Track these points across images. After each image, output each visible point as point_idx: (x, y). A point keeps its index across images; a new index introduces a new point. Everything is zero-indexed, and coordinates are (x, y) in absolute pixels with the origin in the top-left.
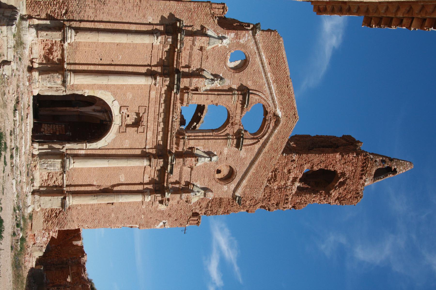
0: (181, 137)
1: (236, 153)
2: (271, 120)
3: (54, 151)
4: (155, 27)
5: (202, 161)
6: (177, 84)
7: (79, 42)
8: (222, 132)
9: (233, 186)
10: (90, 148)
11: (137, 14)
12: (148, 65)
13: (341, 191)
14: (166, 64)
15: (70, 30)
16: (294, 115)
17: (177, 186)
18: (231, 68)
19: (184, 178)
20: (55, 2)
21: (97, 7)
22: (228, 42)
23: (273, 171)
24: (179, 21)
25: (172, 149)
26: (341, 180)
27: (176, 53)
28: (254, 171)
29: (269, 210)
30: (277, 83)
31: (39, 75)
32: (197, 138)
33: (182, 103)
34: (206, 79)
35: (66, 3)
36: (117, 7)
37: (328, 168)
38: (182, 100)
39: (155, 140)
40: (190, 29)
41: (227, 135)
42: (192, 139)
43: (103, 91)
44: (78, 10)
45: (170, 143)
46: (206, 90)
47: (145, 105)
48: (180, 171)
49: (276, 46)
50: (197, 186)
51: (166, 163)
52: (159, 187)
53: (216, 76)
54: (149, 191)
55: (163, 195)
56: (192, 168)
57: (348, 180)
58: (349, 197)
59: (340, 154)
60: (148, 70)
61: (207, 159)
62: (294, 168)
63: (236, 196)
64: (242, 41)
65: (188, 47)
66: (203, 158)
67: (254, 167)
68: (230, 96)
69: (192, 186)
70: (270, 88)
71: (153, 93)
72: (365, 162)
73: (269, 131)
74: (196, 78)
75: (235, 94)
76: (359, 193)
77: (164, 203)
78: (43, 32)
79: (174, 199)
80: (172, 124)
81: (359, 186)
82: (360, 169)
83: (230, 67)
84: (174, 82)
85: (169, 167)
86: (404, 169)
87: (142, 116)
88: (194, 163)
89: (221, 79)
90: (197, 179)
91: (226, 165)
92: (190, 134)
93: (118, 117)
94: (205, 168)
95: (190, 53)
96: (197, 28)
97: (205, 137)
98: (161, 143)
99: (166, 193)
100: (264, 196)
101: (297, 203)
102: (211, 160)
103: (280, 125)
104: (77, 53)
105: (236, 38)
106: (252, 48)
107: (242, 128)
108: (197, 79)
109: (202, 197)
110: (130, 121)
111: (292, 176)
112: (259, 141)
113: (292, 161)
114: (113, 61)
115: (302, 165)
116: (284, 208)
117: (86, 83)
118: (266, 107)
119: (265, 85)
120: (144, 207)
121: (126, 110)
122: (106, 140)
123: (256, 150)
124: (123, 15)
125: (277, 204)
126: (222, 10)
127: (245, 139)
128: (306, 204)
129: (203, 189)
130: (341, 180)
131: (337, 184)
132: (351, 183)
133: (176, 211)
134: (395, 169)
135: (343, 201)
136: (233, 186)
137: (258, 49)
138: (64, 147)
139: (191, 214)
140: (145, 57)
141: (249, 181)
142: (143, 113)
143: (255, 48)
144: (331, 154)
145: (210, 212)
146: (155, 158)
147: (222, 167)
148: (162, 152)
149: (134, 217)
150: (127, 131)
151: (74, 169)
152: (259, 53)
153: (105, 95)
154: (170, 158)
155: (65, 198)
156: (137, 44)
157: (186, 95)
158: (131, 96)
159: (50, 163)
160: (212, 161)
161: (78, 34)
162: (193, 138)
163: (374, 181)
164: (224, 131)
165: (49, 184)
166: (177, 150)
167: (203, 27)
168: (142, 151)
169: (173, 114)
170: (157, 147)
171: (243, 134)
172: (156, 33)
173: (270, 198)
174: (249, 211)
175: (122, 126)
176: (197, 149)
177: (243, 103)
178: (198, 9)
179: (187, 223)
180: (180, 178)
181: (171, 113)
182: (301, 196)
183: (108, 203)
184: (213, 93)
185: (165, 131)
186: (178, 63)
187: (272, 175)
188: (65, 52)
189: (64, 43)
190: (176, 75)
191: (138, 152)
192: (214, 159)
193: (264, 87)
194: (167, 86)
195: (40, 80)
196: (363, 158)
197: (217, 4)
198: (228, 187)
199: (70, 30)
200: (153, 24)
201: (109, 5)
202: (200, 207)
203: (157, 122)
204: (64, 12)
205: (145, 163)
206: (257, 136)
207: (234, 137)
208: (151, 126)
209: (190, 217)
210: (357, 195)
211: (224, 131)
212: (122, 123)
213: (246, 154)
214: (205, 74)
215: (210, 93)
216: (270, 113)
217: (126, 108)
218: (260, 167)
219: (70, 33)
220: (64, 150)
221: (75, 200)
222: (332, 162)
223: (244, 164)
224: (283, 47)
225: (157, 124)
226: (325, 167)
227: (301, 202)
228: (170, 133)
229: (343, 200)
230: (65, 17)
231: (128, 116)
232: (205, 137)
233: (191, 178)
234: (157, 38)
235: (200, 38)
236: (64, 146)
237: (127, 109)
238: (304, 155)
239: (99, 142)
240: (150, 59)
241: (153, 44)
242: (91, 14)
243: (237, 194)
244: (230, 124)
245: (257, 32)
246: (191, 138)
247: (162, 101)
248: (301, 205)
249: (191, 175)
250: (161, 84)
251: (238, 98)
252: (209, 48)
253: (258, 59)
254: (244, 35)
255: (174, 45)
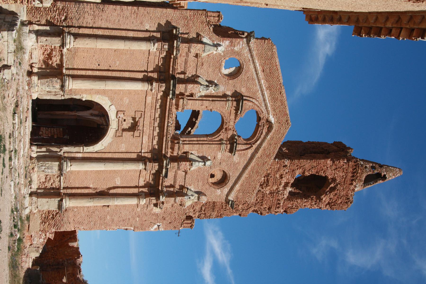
0: (176, 141)
1: (229, 157)
2: (264, 126)
3: (51, 154)
4: (152, 34)
5: (197, 166)
6: (172, 90)
7: (78, 48)
8: (216, 138)
9: (226, 190)
10: (87, 151)
11: (135, 21)
12: (145, 71)
13: (332, 196)
14: (162, 70)
15: (69, 36)
16: (287, 121)
17: (172, 189)
18: (226, 75)
19: (178, 182)
20: (55, 9)
21: (95, 14)
22: (223, 49)
23: (266, 176)
24: (176, 28)
25: (167, 153)
26: (332, 185)
27: (172, 60)
28: (247, 176)
29: (261, 214)
30: (270, 90)
31: (38, 79)
32: (192, 142)
33: (177, 109)
34: (201, 85)
35: (66, 10)
36: (115, 14)
37: (320, 174)
38: (177, 105)
39: (151, 145)
40: (186, 36)
41: (221, 140)
42: (186, 144)
43: (100, 96)
44: (77, 17)
45: (165, 147)
46: (201, 96)
47: (141, 110)
48: (174, 175)
49: (270, 54)
50: (191, 190)
51: (161, 167)
52: (153, 190)
53: (211, 82)
54: (144, 194)
55: (158, 198)
56: (186, 173)
57: (339, 185)
58: (339, 202)
59: (331, 160)
60: (144, 75)
61: (201, 163)
62: (286, 173)
63: (229, 200)
64: (236, 49)
65: (184, 54)
66: (197, 163)
67: (247, 172)
68: (224, 102)
69: (186, 190)
70: (263, 95)
71: (149, 99)
72: (356, 168)
73: (262, 136)
74: (191, 84)
75: (229, 100)
76: (349, 199)
77: (159, 206)
78: (42, 38)
79: (168, 203)
80: (167, 129)
81: (350, 192)
82: (350, 175)
83: (225, 73)
84: (170, 88)
85: (164, 170)
86: (394, 175)
87: (138, 121)
88: (189, 167)
89: (216, 85)
90: (192, 183)
91: (220, 170)
92: (185, 139)
93: (115, 121)
94: (199, 172)
95: (186, 59)
96: (193, 35)
97: (200, 142)
98: (157, 148)
99: (161, 197)
100: (257, 200)
101: (289, 207)
102: (205, 165)
103: (273, 131)
104: (76, 58)
105: (231, 45)
106: (246, 55)
107: (235, 133)
108: (192, 85)
109: (196, 201)
110: (126, 125)
111: (284, 181)
112: (252, 146)
113: (284, 166)
114: (110, 66)
115: (293, 170)
116: (276, 212)
117: (83, 88)
118: (259, 113)
119: (258, 91)
120: (139, 210)
121: (122, 115)
122: (103, 143)
123: (249, 155)
124: (120, 22)
125: (269, 209)
126: (217, 18)
127: (239, 144)
128: (297, 208)
129: (196, 192)
130: (332, 185)
131: (328, 189)
132: (342, 188)
133: (170, 214)
134: (385, 175)
135: (334, 206)
136: (226, 190)
137: (252, 56)
138: (61, 150)
139: (185, 217)
140: (142, 63)
141: (242, 185)
142: (140, 118)
143: (249, 55)
144: (322, 160)
145: (203, 216)
146: (150, 162)
147: (216, 172)
148: (157, 156)
149: (129, 219)
150: (123, 135)
151: (71, 172)
152: (253, 60)
153: (102, 99)
154: (165, 162)
155: (61, 200)
156: (134, 50)
157: (181, 101)
158: (127, 101)
159: (47, 165)
160: (206, 165)
161: (77, 40)
162: (188, 142)
163: (364, 186)
164: (218, 136)
165: (46, 187)
166: (172, 155)
167: (198, 35)
168: (138, 155)
169: (168, 119)
170: (153, 151)
171: (236, 139)
172: (153, 40)
173: (262, 202)
174: (242, 215)
175: (118, 130)
176: (191, 154)
177: (237, 109)
178: (194, 17)
179: (181, 226)
180: (175, 182)
181: (167, 118)
182: (292, 201)
183: (104, 206)
184: (208, 99)
185: (161, 135)
186: (174, 69)
187: (264, 180)
188: (64, 57)
189: (63, 48)
190: (172, 81)
191: (134, 156)
192: (208, 163)
193: (258, 94)
194: (163, 91)
195: (39, 85)
196: (353, 164)
197: (213, 12)
198: (221, 192)
199: (69, 36)
200: (150, 31)
201: (107, 12)
202: (194, 211)
203: (153, 127)
204: (63, 18)
205: (141, 166)
206: (251, 142)
207: (228, 143)
208: (147, 130)
209: (184, 220)
210: (348, 201)
211: (218, 136)
212: (118, 127)
213: (239, 159)
214: (200, 80)
215: (204, 99)
216: (263, 119)
217: (122, 113)
218: (253, 172)
219: (69, 39)
220: (61, 153)
221: (71, 202)
222: (324, 168)
223: (237, 169)
224: (276, 55)
225: (152, 128)
226: (317, 173)
227: (292, 206)
228: (165, 138)
229: (334, 205)
230: (64, 23)
231: (125, 120)
232: (200, 142)
233: (185, 182)
234: (154, 45)
235: (196, 45)
236: (62, 149)
237: (124, 114)
238: (296, 161)
239: (95, 145)
240: (147, 65)
241: (149, 50)
242: (89, 21)
243: (231, 198)
244: (224, 130)
245: (252, 39)
246: (185, 142)
247: (158, 107)
248: (293, 210)
249: (185, 179)
250: (158, 89)
251: (232, 104)
252: (204, 55)
253: (252, 66)
254: (239, 43)
255: (170, 52)
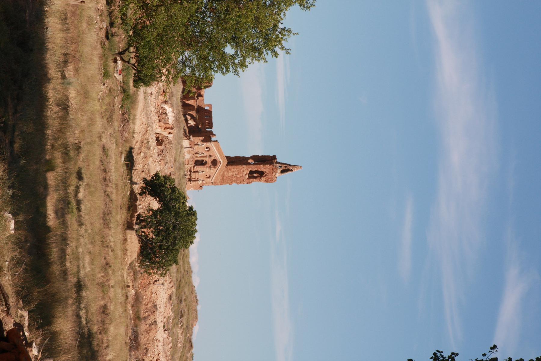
5: (200, 173)
9: (210, 179)
53: (202, 153)
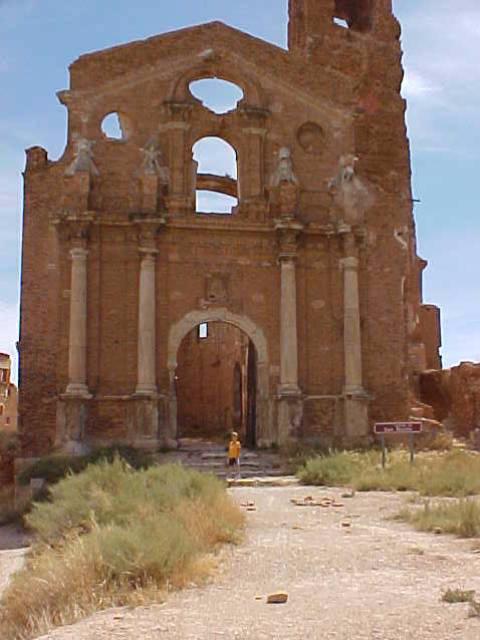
28: (308, 89)
88: (290, 185)
155: (350, 396)
